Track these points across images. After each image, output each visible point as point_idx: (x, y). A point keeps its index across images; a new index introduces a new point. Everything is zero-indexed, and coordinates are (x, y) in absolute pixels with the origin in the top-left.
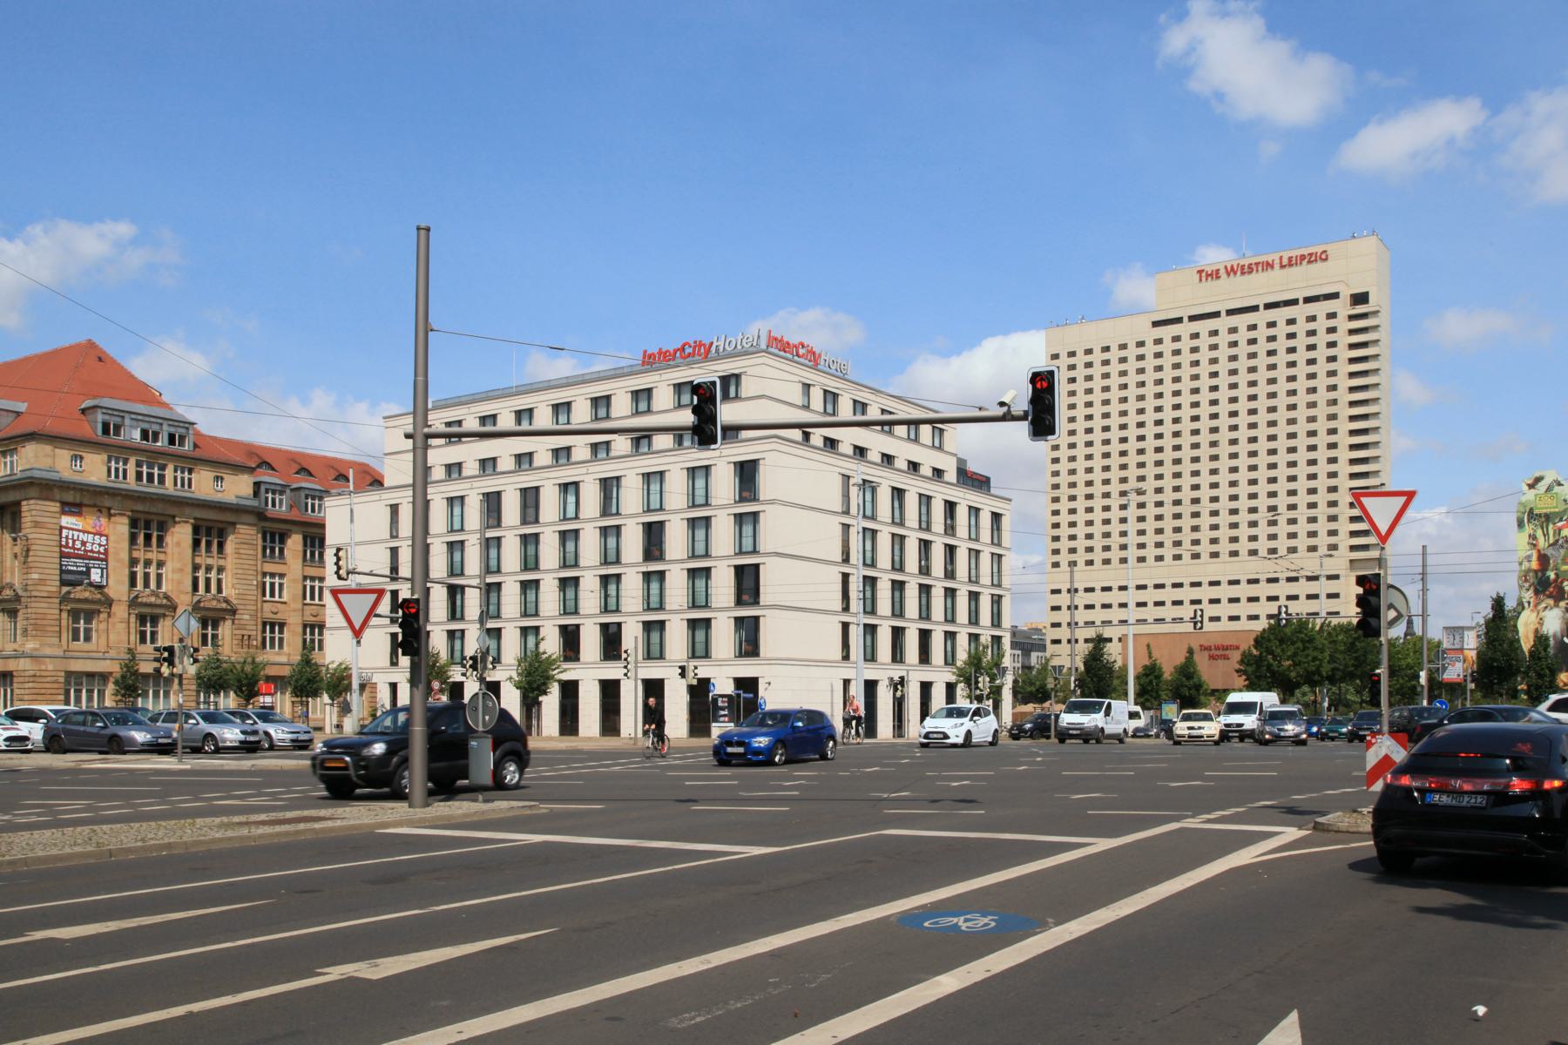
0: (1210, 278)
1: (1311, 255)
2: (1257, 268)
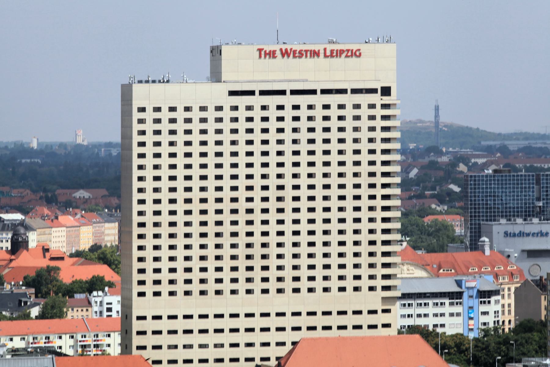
0: (268, 57)
1: (348, 50)
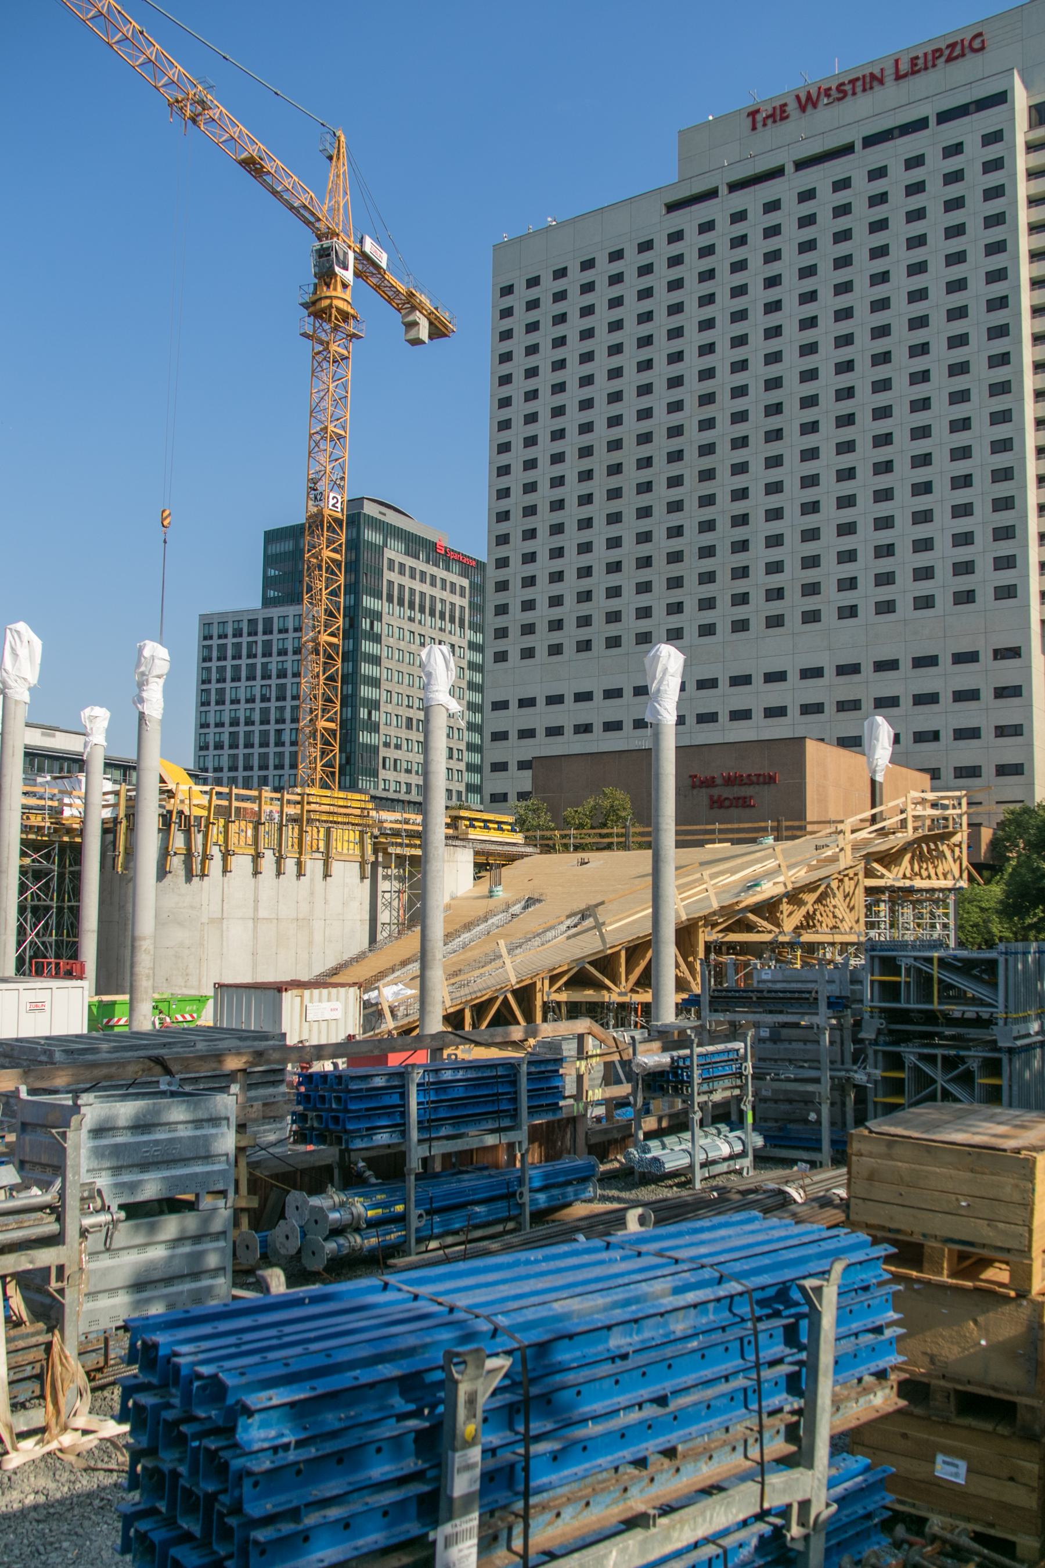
2: (854, 89)
